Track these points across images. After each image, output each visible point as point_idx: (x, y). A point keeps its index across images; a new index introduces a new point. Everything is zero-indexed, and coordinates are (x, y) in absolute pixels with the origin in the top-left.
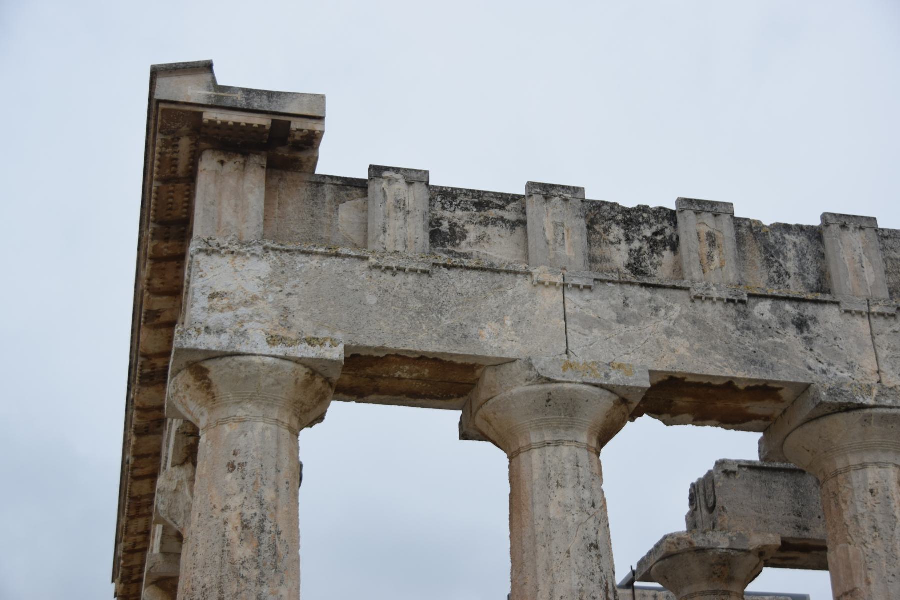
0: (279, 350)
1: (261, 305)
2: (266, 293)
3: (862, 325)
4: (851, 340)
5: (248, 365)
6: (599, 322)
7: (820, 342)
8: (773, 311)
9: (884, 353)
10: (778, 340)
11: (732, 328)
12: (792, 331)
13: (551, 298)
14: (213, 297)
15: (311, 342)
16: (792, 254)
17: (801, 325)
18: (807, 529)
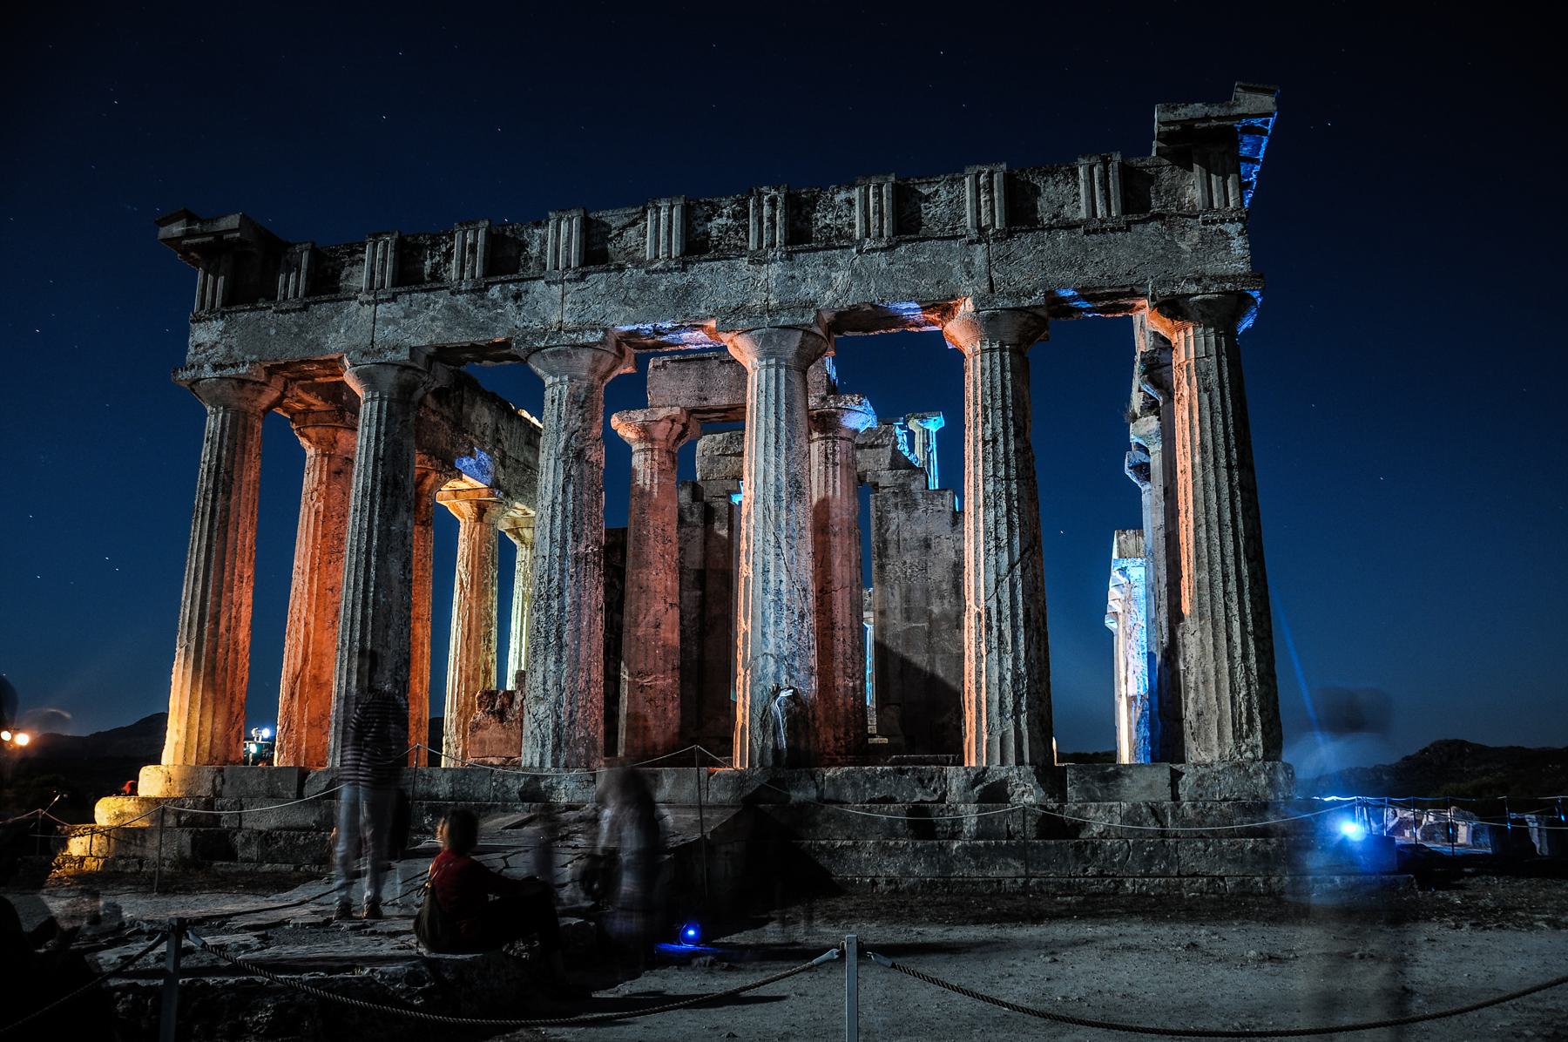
0: (219, 373)
1: (219, 346)
2: (221, 339)
3: (556, 290)
4: (547, 302)
5: (206, 384)
6: (394, 321)
7: (526, 307)
8: (501, 290)
9: (567, 306)
10: (499, 311)
11: (471, 308)
12: (510, 304)
13: (367, 310)
14: (197, 346)
15: (232, 366)
16: (536, 243)
17: (517, 297)
18: (706, 399)
